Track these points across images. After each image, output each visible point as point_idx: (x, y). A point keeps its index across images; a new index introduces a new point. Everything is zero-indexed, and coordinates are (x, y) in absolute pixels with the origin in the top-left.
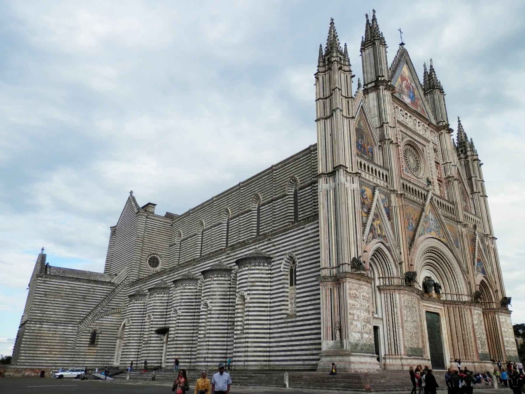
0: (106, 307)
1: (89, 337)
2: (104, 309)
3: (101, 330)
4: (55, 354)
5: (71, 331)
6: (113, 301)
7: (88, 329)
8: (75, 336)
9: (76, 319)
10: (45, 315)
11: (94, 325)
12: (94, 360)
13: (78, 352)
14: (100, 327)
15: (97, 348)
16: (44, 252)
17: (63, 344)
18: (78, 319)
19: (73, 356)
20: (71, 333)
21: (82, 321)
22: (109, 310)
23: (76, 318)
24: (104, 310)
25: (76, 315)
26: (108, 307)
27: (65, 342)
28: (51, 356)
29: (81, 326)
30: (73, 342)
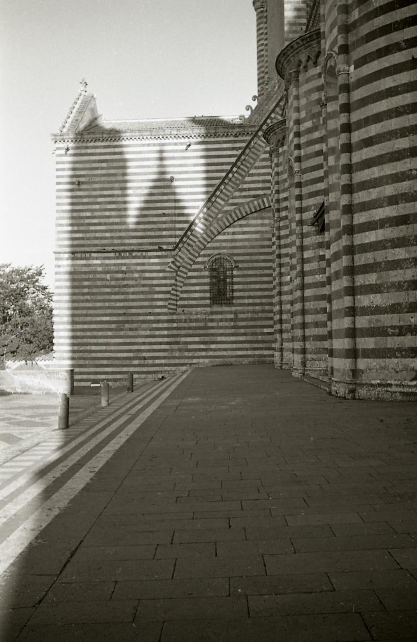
0: (237, 194)
1: (207, 281)
2: (231, 201)
3: (235, 258)
4: (131, 329)
5: (158, 268)
6: (252, 175)
7: (200, 259)
8: (173, 282)
9: (165, 237)
10: (88, 235)
11: (214, 248)
12: (232, 338)
13: (186, 321)
14: (230, 251)
15: (233, 309)
16: (91, 90)
17: (146, 304)
18: (171, 236)
19: (175, 332)
20: (161, 275)
21: (181, 241)
22: (248, 203)
23: (164, 233)
24: (232, 204)
25: (164, 226)
26: (244, 193)
27: (149, 297)
28: (122, 333)
29: (180, 253)
30: (168, 296)
